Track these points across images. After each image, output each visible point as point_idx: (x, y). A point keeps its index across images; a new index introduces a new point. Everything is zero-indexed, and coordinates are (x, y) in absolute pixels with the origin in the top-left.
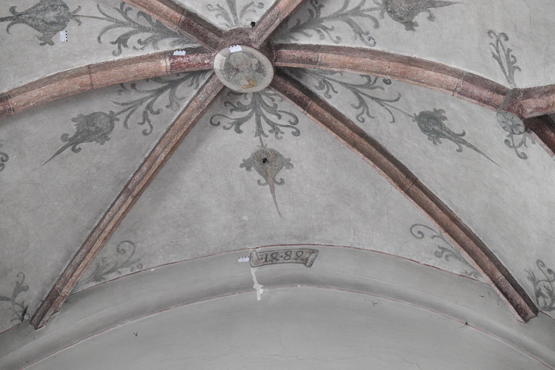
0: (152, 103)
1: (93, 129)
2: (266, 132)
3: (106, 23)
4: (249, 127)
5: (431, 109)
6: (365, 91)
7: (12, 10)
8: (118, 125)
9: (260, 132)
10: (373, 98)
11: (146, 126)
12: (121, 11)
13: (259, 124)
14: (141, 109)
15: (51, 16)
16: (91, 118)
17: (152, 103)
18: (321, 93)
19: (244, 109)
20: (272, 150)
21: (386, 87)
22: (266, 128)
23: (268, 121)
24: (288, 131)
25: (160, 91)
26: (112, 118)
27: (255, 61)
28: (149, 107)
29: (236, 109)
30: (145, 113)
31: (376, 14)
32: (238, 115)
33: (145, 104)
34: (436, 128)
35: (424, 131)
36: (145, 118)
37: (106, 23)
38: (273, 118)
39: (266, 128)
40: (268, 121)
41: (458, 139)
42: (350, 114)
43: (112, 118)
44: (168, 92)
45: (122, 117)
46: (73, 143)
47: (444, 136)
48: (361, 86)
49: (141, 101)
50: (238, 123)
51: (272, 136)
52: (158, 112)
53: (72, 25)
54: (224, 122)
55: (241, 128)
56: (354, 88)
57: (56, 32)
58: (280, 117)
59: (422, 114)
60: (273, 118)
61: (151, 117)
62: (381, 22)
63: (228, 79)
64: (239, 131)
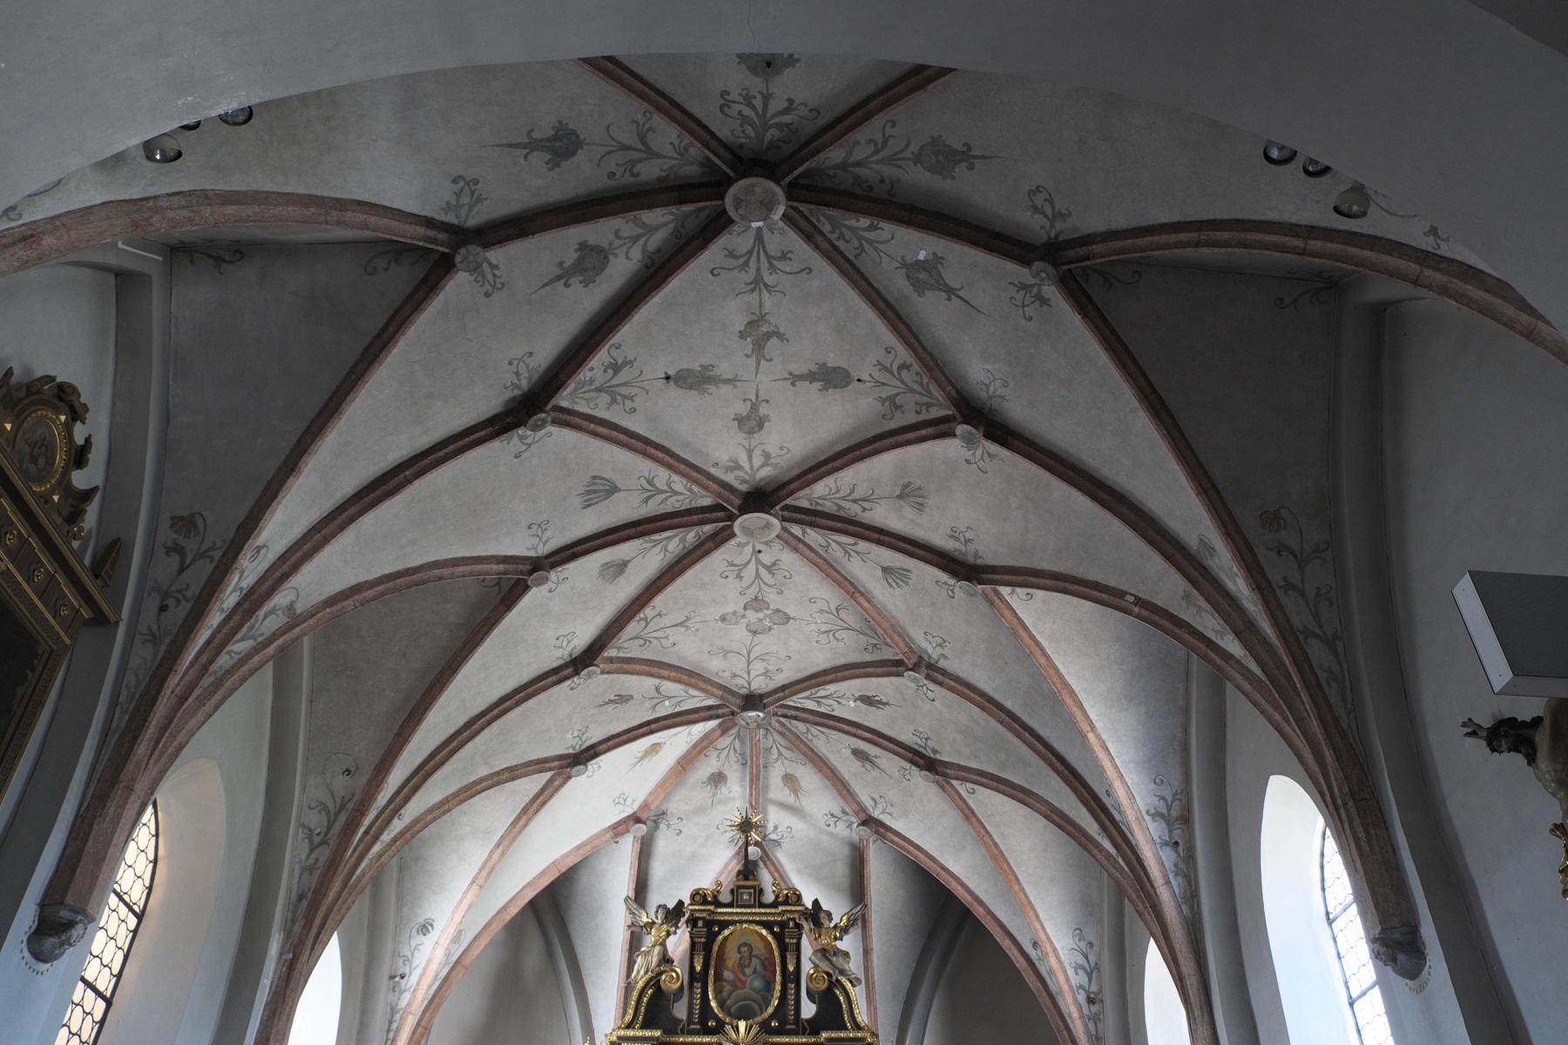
0: (872, 155)
1: (941, 158)
2: (759, 97)
3: (881, 247)
4: (777, 104)
5: (563, 164)
6: (637, 155)
7: (949, 299)
8: (915, 147)
9: (767, 98)
10: (630, 148)
11: (889, 131)
12: (863, 250)
13: (765, 107)
14: (885, 153)
15: (923, 276)
16: (940, 170)
17: (872, 155)
18: (688, 139)
19: (778, 125)
20: (756, 74)
21: (613, 168)
22: (758, 102)
23: (754, 108)
24: (734, 96)
25: (858, 164)
26: (917, 158)
27: (741, 211)
28: (877, 152)
29: (786, 125)
30: (883, 148)
31: (617, 243)
32: (786, 119)
33: (880, 156)
34: (558, 144)
35: (574, 133)
36: (885, 142)
37: (881, 247)
38: (747, 112)
39: (758, 102)
40: (754, 108)
41: (532, 146)
42: (658, 120)
43: (917, 158)
44: (852, 160)
45: (907, 154)
46: (965, 156)
47: (548, 140)
48: (641, 160)
49: (880, 162)
50: (786, 111)
51: (753, 92)
52: (871, 141)
53: (909, 259)
54: (804, 111)
55: (786, 104)
56: (651, 154)
57: (925, 261)
58: (740, 113)
59: (573, 153)
60: (747, 112)
61: (880, 141)
62: (611, 237)
63: (774, 193)
64: (790, 101)
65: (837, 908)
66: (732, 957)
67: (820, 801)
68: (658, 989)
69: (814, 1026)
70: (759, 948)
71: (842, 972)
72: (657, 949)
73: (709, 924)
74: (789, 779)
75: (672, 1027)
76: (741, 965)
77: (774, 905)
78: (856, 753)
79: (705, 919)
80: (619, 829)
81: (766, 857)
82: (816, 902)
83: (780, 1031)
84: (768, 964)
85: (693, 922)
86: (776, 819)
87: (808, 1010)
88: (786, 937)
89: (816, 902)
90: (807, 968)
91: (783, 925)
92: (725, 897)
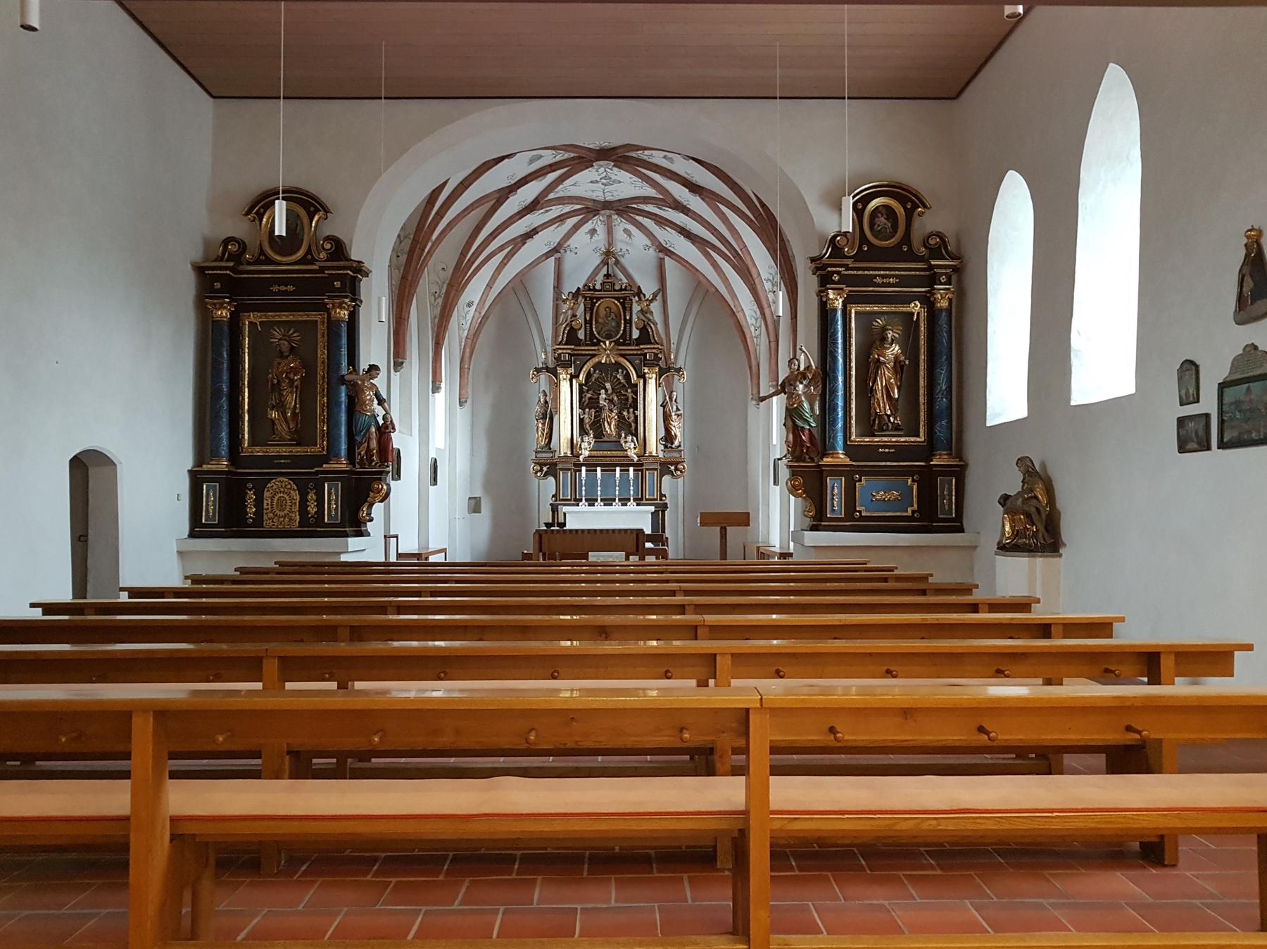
65: (649, 288)
66: (602, 312)
67: (640, 239)
68: (572, 328)
69: (639, 341)
70: (614, 309)
72: (570, 312)
73: (591, 299)
74: (626, 231)
75: (578, 342)
76: (607, 317)
77: (621, 290)
79: (588, 295)
80: (548, 255)
81: (617, 262)
84: (618, 316)
85: (585, 298)
86: (618, 247)
87: (636, 334)
88: (625, 303)
90: (635, 319)
91: (625, 298)
92: (598, 287)
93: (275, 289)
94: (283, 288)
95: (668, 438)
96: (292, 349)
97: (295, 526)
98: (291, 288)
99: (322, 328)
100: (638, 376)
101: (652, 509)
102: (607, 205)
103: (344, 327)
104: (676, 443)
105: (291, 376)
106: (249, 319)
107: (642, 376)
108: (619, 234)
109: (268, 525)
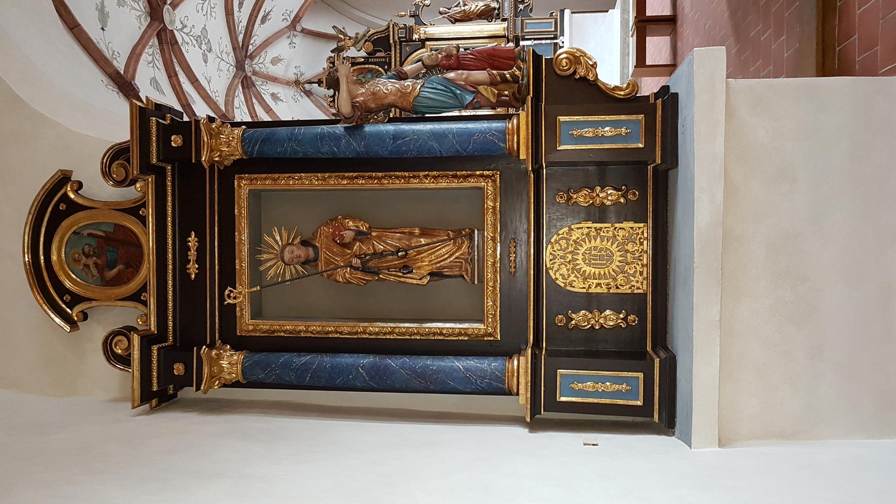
71: (365, 36)
74: (275, 61)
78: (263, 22)
82: (332, 51)
83: (390, 65)
84: (361, 72)
89: (332, 51)
93: (193, 269)
94: (192, 254)
95: (487, 14)
96: (305, 243)
97: (644, 230)
98: (192, 241)
99: (265, 182)
100: (423, 47)
101: (567, 12)
102: (240, 66)
103: (252, 131)
104: (494, 5)
105: (348, 235)
106: (247, 323)
107: (423, 42)
108: (277, 71)
109: (638, 282)
